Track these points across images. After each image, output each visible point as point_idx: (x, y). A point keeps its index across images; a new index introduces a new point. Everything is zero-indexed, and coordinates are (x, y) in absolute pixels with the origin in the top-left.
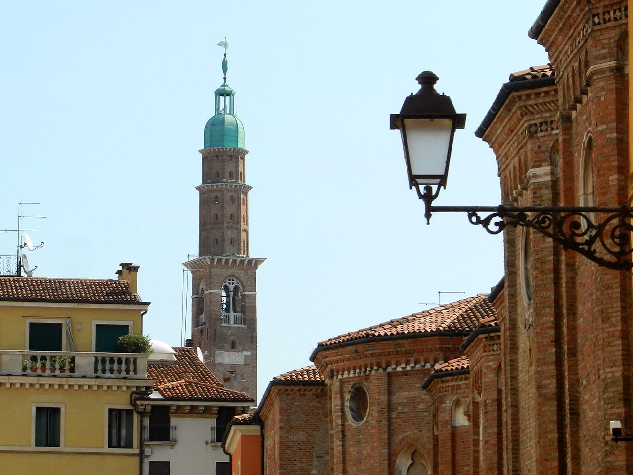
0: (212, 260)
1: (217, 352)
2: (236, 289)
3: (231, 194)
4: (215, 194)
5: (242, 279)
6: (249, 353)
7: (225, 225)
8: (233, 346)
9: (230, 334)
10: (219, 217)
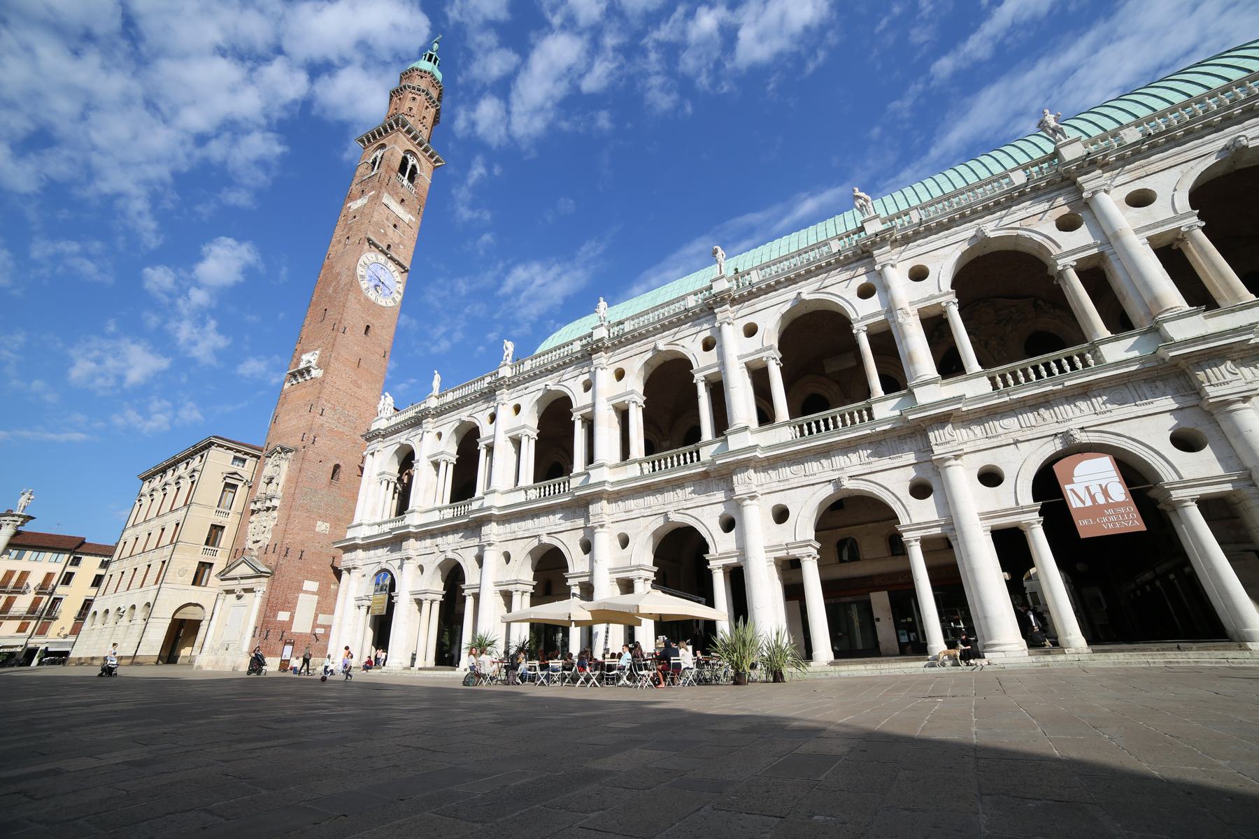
2: (414, 166)
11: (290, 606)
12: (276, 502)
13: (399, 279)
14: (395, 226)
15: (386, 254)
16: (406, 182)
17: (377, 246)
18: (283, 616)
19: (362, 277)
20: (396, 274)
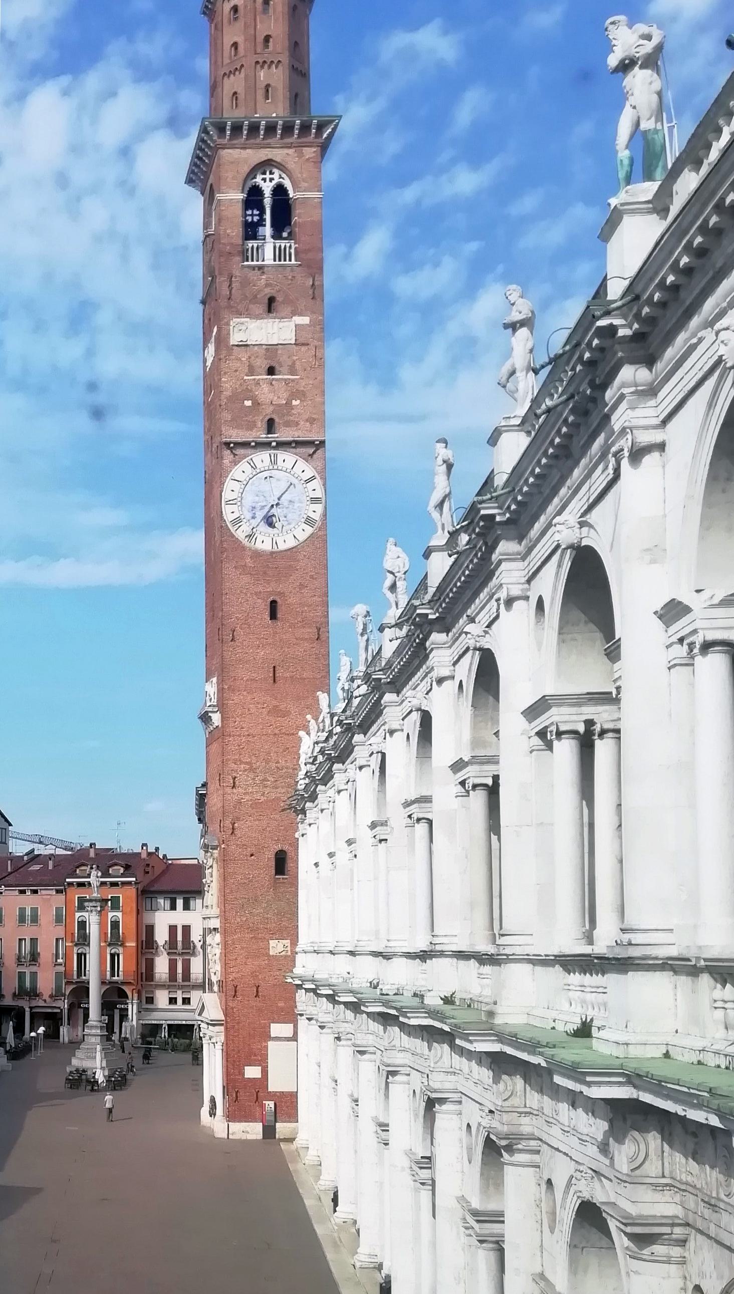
0: (221, 129)
1: (235, 321)
2: (280, 190)
5: (291, 165)
6: (305, 320)
8: (271, 305)
9: (263, 282)
11: (262, 1062)
12: (216, 923)
13: (310, 472)
14: (271, 371)
15: (266, 445)
17: (245, 445)
18: (252, 1072)
19: (237, 521)
20: (302, 464)
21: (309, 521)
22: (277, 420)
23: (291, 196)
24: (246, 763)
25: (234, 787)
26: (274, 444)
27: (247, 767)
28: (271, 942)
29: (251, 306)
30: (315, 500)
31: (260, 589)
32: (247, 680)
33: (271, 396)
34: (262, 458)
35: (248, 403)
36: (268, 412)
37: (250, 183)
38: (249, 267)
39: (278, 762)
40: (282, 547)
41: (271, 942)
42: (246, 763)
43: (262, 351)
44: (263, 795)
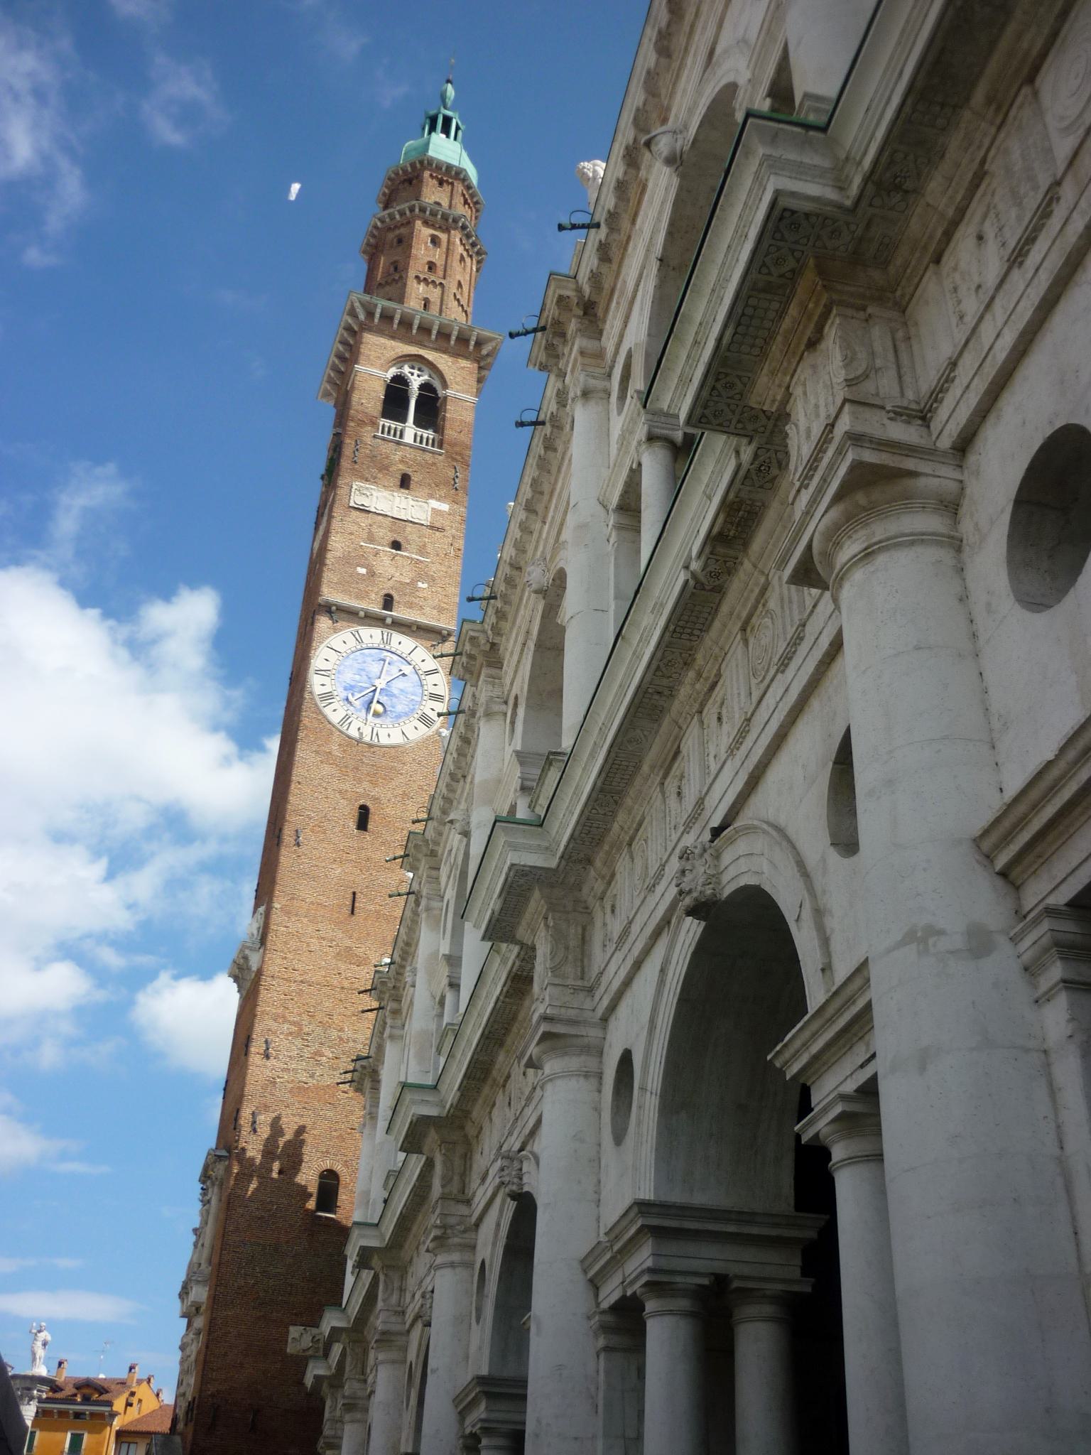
0: (370, 314)
2: (425, 387)
3: (432, 232)
4: (397, 232)
6: (445, 507)
7: (412, 273)
8: (405, 482)
9: (397, 458)
10: (400, 267)
14: (396, 545)
16: (410, 431)
19: (328, 696)
21: (425, 720)
22: (396, 597)
23: (441, 393)
24: (294, 1023)
25: (267, 1057)
26: (389, 621)
27: (294, 1029)
28: (292, 1329)
29: (380, 475)
30: (436, 697)
31: (346, 786)
32: (312, 903)
33: (392, 571)
34: (372, 635)
35: (362, 571)
36: (387, 588)
37: (393, 371)
38: (383, 439)
39: (341, 1030)
40: (384, 741)
41: (292, 1329)
42: (294, 1023)
43: (387, 521)
44: (312, 1076)
